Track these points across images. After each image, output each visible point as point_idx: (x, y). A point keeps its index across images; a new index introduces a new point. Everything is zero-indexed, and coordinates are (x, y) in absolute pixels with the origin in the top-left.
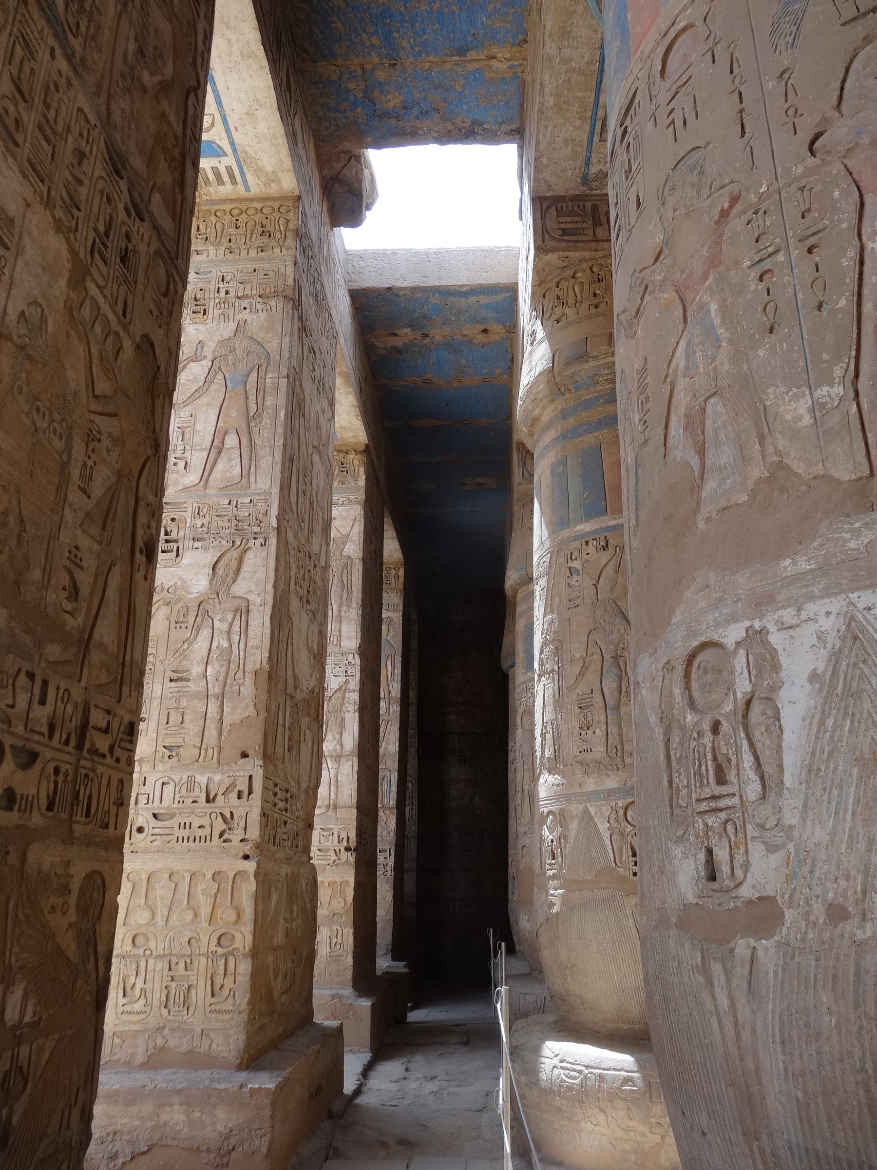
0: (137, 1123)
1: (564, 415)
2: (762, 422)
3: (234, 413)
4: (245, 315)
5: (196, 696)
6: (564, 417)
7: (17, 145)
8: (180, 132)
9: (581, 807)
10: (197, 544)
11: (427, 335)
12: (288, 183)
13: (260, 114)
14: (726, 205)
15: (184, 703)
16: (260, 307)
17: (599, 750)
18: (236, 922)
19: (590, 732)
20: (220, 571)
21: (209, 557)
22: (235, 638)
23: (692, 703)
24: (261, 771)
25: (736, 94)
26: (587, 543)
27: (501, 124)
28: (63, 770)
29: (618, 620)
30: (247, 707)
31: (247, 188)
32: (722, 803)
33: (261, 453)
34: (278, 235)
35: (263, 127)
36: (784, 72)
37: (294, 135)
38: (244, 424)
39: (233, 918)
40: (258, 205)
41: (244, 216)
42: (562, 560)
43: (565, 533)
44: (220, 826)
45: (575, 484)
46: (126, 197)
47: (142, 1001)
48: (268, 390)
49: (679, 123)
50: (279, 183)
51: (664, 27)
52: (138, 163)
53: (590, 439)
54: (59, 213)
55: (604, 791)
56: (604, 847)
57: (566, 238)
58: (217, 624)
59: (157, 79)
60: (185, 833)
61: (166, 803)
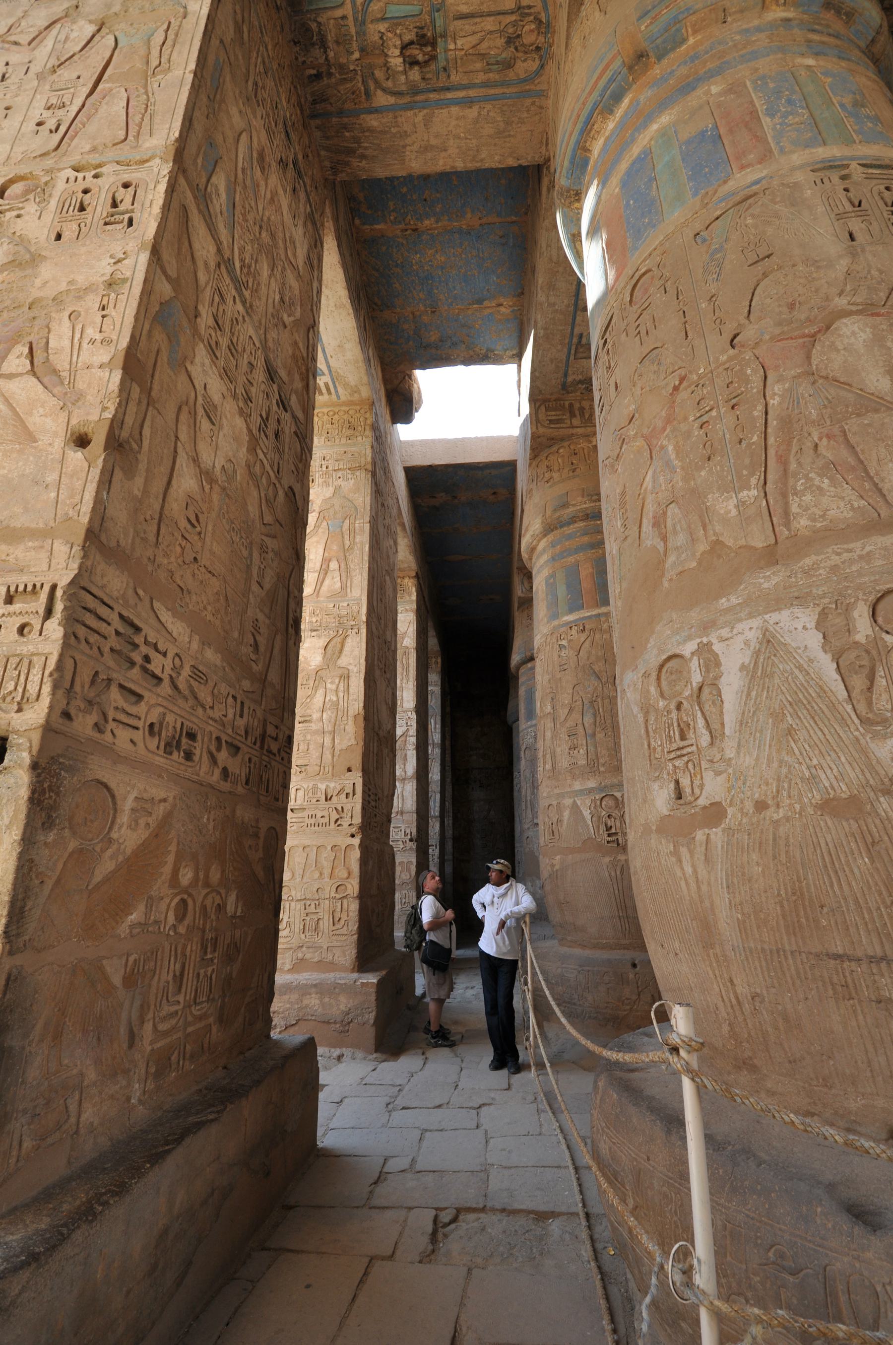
0: (288, 1006)
1: (553, 545)
2: (705, 516)
3: (335, 548)
4: (340, 482)
5: (316, 732)
6: (553, 546)
7: (217, 358)
8: (305, 355)
9: (571, 801)
10: (314, 634)
11: (456, 498)
12: (365, 392)
13: (348, 346)
14: (677, 383)
15: (309, 737)
16: (349, 476)
17: (583, 762)
18: (347, 878)
19: (576, 752)
21: (322, 642)
23: (662, 695)
24: (361, 780)
25: (681, 312)
26: (571, 628)
27: (506, 350)
28: (253, 761)
29: (593, 678)
30: (350, 739)
31: (338, 397)
32: (684, 751)
33: (353, 574)
34: (360, 428)
35: (349, 355)
36: (712, 297)
37: (369, 360)
38: (342, 554)
39: (346, 875)
40: (346, 409)
41: (336, 416)
42: (554, 640)
43: (556, 623)
44: (335, 816)
45: (562, 591)
46: (277, 396)
47: (288, 930)
48: (357, 531)
49: (643, 332)
50: (360, 394)
51: (631, 273)
52: (283, 373)
53: (571, 559)
54: (241, 404)
55: (586, 789)
56: (587, 826)
57: (553, 426)
58: (329, 686)
59: (292, 319)
60: (313, 821)
61: (299, 802)
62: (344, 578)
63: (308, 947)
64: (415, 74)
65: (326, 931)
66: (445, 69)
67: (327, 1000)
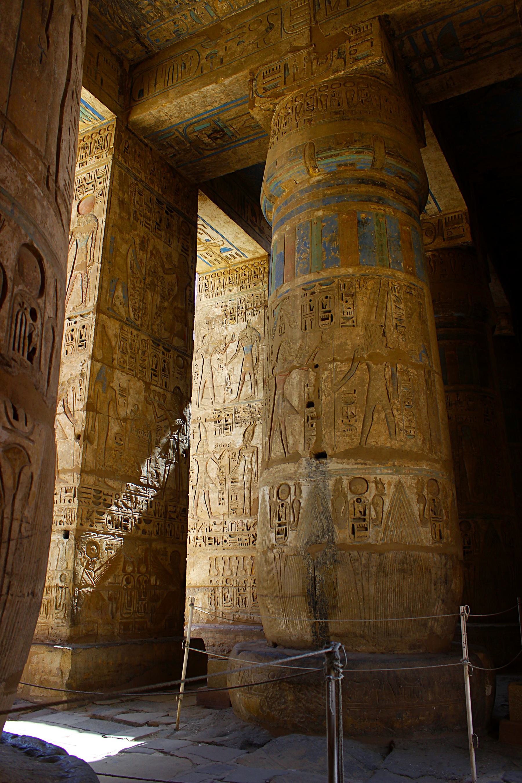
3: (248, 365)
4: (250, 318)
5: (240, 488)
10: (237, 425)
15: (237, 491)
16: (255, 313)
20: (246, 436)
21: (242, 430)
22: (253, 464)
31: (247, 257)
33: (259, 382)
34: (261, 276)
38: (252, 369)
41: (247, 269)
48: (260, 352)
58: (246, 458)
60: (240, 542)
61: (233, 531)
62: (253, 386)
63: (241, 612)
64: (219, 141)
65: (249, 604)
66: (233, 136)
67: (247, 639)
